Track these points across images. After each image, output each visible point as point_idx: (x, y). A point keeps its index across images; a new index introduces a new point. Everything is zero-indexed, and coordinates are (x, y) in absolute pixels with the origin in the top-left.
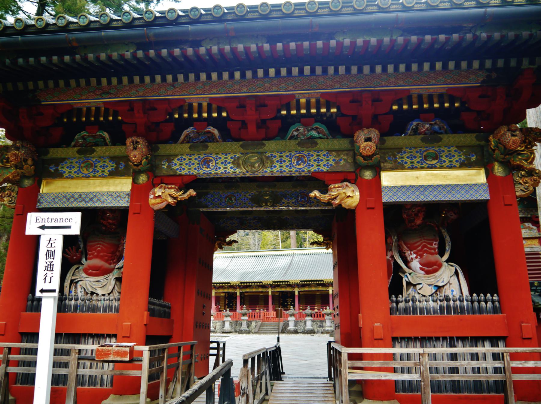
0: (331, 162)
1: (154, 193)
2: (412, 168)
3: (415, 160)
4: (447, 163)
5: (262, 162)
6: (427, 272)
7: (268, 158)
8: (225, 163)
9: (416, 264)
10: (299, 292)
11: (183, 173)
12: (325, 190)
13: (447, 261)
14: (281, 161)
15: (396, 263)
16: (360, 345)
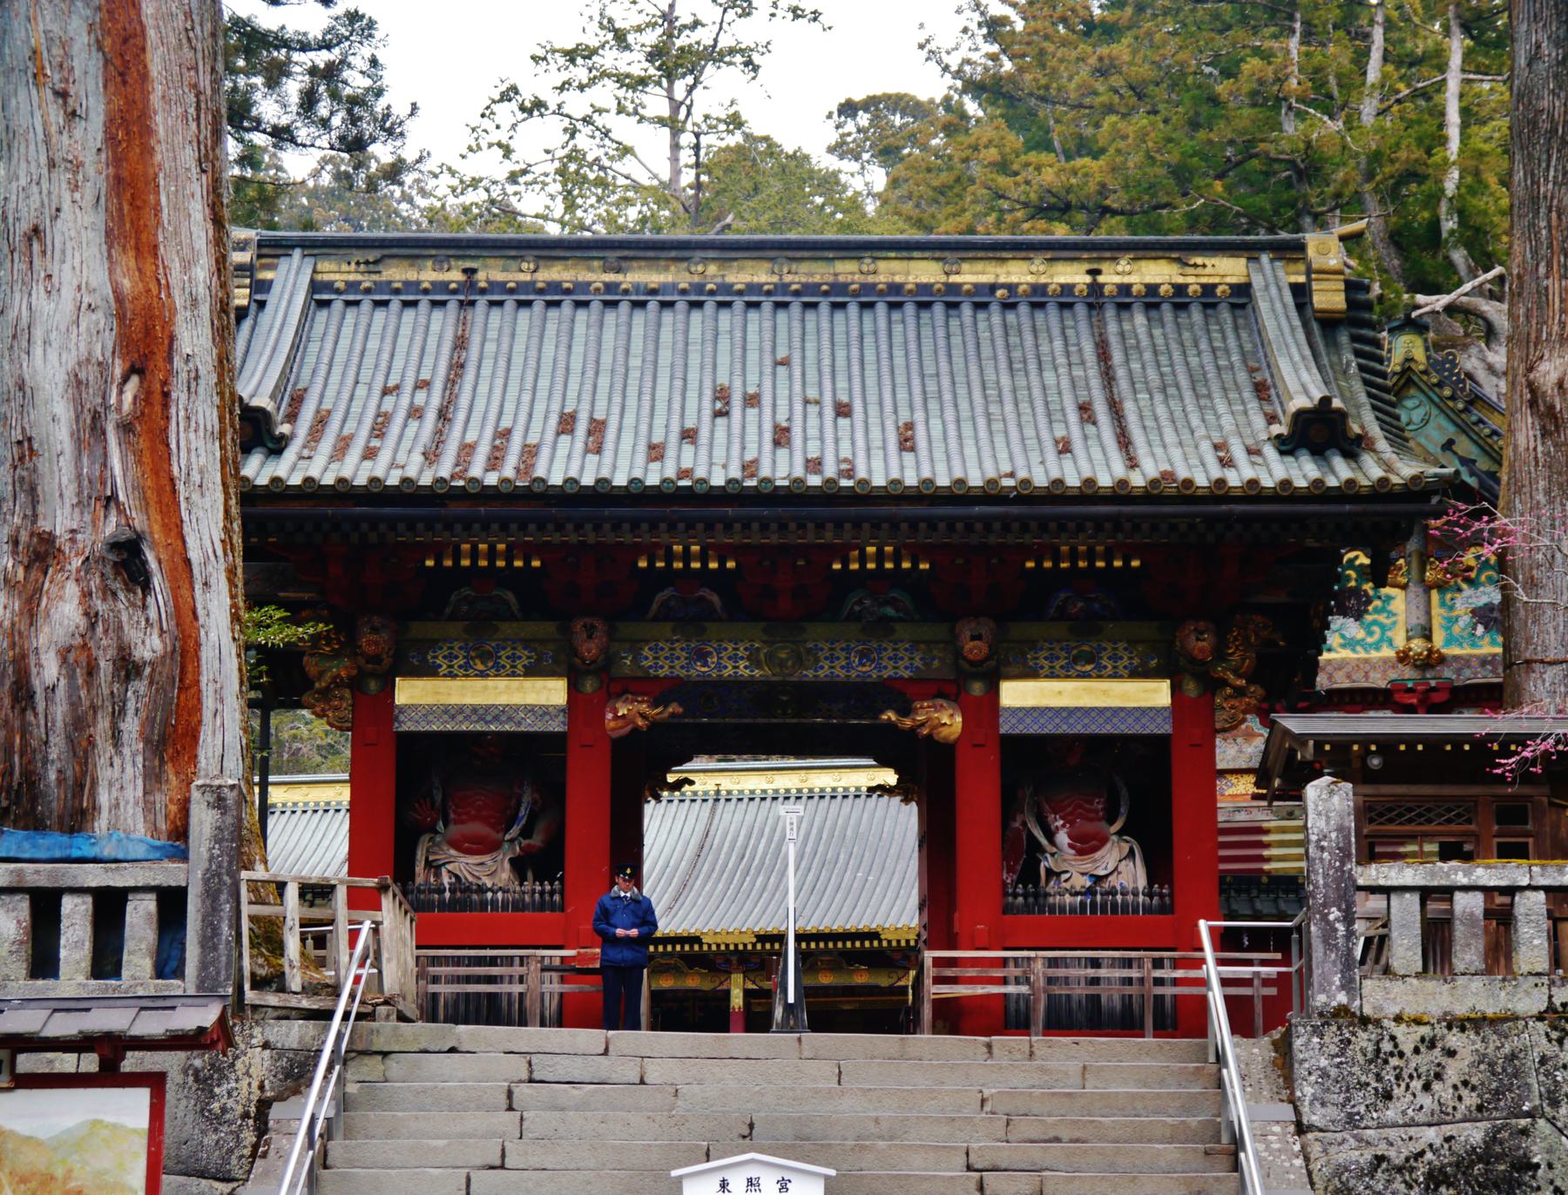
0: (918, 663)
1: (615, 711)
2: (1052, 676)
3: (1058, 664)
4: (1109, 670)
5: (800, 662)
6: (1080, 852)
7: (809, 651)
8: (735, 658)
9: (1063, 838)
10: (748, 994)
11: (661, 673)
12: (905, 711)
13: (1120, 833)
14: (832, 658)
15: (1031, 837)
16: (953, 946)
